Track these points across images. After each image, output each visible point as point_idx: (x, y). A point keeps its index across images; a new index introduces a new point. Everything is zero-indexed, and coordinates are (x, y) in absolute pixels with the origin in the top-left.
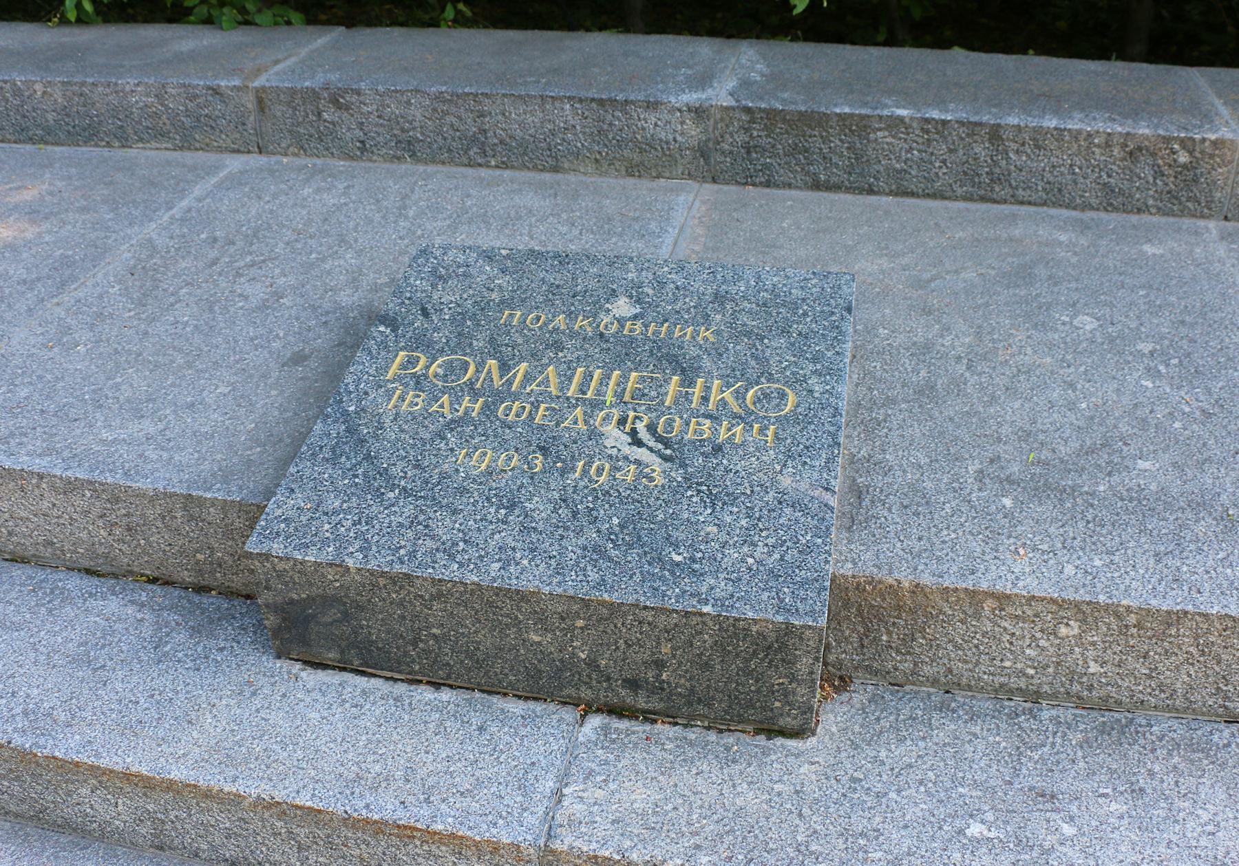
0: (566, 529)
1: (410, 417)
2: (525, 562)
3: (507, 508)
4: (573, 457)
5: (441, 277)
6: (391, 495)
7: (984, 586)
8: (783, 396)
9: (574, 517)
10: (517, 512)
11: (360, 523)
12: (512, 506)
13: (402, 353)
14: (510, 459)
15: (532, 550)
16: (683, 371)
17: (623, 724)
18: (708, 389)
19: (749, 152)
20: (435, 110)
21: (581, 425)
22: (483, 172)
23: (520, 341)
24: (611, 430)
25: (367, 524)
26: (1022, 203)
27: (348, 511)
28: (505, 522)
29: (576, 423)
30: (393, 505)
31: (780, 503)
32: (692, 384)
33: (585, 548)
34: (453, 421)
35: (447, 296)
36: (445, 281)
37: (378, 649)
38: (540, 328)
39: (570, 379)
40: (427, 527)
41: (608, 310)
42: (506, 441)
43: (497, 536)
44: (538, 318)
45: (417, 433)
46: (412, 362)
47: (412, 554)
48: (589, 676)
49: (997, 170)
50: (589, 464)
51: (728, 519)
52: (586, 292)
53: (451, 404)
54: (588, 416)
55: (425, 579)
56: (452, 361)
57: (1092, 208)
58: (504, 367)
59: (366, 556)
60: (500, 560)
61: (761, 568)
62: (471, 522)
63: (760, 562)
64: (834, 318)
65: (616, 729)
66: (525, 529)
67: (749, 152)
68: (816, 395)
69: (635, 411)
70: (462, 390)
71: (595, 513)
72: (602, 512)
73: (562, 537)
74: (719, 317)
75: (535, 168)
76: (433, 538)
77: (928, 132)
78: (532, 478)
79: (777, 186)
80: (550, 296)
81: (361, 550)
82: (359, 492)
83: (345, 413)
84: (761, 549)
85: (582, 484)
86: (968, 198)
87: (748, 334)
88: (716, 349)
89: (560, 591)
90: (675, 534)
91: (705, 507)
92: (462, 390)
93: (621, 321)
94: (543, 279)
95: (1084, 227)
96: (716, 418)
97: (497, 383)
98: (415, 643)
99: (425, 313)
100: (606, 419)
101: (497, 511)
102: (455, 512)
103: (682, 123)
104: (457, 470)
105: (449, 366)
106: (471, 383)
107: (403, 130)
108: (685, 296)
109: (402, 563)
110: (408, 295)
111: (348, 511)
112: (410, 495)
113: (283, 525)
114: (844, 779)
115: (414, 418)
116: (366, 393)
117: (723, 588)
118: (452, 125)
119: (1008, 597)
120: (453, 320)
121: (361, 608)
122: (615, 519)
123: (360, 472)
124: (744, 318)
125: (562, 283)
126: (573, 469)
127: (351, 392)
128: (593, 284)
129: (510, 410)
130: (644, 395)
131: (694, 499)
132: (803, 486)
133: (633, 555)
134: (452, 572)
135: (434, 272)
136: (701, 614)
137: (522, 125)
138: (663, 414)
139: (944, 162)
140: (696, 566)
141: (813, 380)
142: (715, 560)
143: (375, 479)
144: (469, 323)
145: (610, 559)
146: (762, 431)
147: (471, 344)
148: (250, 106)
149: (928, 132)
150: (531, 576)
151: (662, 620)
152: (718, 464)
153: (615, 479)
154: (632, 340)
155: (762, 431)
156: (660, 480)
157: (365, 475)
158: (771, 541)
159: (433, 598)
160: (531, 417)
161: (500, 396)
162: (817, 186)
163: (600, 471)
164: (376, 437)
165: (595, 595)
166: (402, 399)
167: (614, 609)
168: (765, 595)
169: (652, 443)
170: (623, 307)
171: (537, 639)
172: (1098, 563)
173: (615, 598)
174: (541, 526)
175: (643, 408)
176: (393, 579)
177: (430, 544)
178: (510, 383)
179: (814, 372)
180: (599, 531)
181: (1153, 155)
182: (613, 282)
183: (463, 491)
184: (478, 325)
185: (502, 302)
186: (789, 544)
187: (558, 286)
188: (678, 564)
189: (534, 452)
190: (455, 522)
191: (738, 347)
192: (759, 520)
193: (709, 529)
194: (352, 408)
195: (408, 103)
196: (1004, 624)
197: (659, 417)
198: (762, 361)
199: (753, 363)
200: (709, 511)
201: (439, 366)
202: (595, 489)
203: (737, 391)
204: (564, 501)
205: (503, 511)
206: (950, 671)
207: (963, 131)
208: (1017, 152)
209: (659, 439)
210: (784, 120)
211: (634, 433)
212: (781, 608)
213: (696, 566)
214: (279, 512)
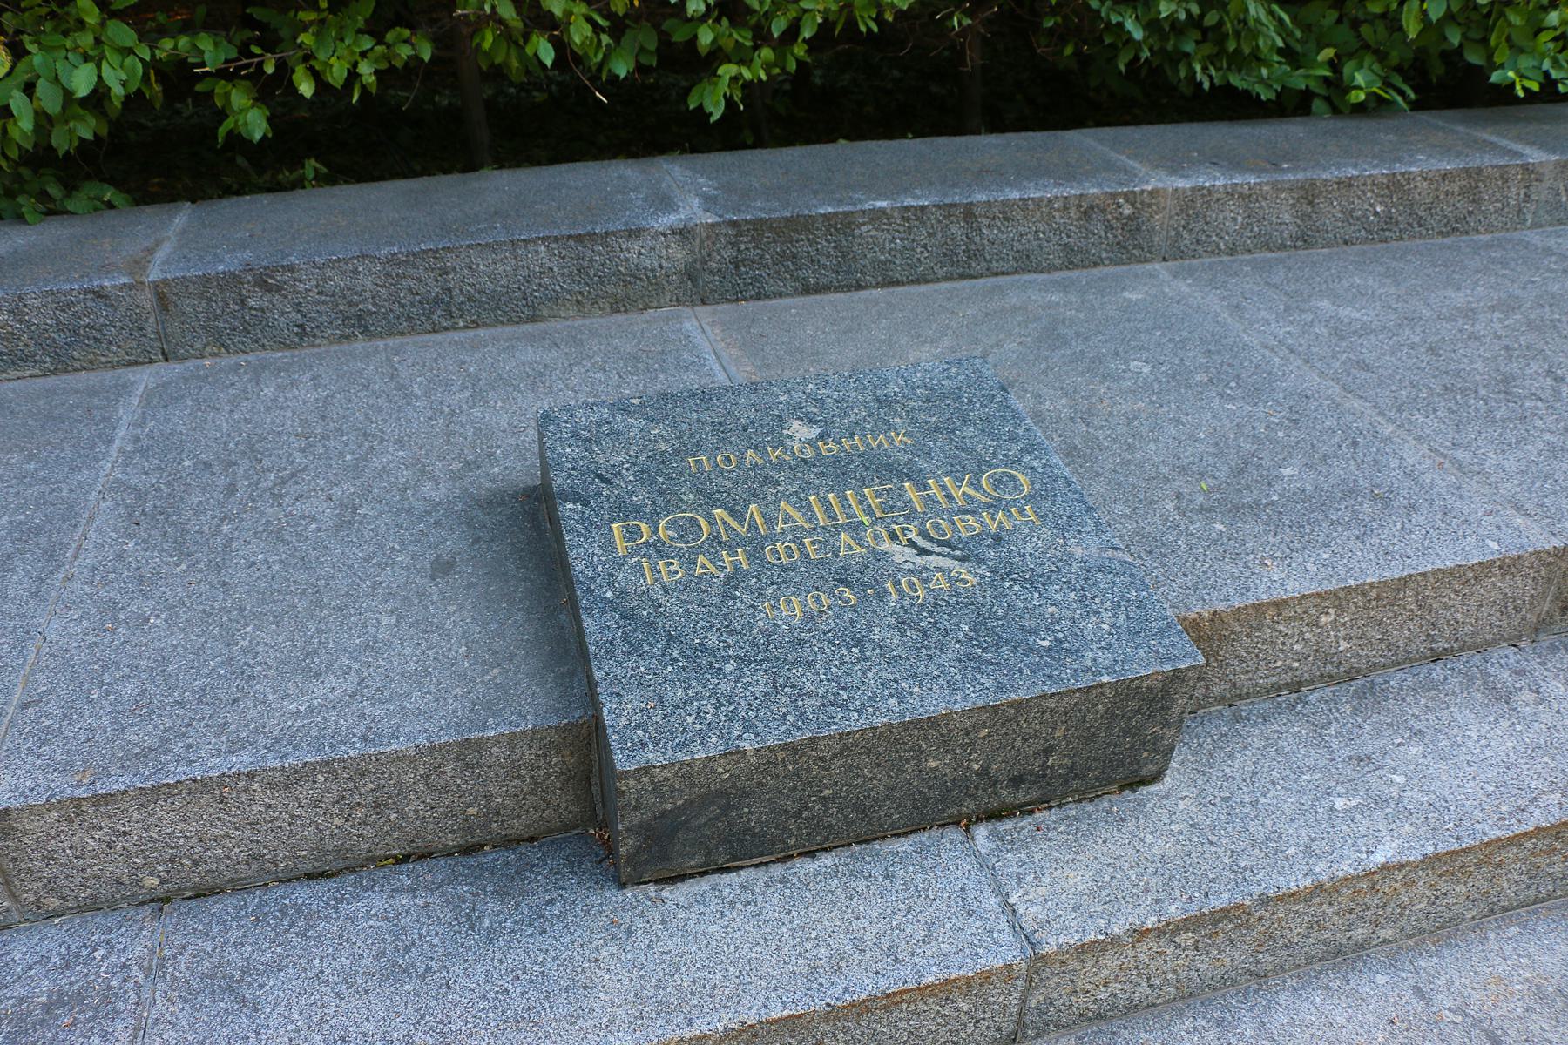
0: (928, 648)
2: (916, 689)
3: (856, 646)
5: (588, 440)
6: (728, 668)
7: (1265, 598)
8: (1013, 478)
13: (614, 526)
14: (818, 599)
15: (915, 677)
16: (910, 479)
17: (1007, 825)
18: (944, 487)
19: (737, 268)
20: (388, 275)
21: (858, 550)
22: (456, 336)
23: (729, 484)
24: (886, 546)
26: (996, 274)
28: (867, 660)
32: (926, 487)
35: (609, 456)
37: (754, 835)
39: (810, 508)
40: (793, 687)
43: (870, 675)
44: (728, 459)
47: (802, 716)
48: (977, 788)
49: (973, 247)
50: (896, 583)
51: (1058, 597)
55: (831, 737)
56: (675, 521)
57: (1057, 269)
58: (739, 516)
59: (757, 735)
60: (891, 696)
63: (1113, 626)
65: (1005, 831)
67: (737, 268)
73: (931, 657)
75: (510, 321)
76: (809, 695)
77: (908, 220)
79: (768, 297)
81: (746, 729)
83: (605, 600)
84: (1106, 616)
86: (948, 278)
87: (937, 430)
89: (969, 705)
90: (1026, 623)
94: (699, 420)
95: (1064, 287)
97: (743, 530)
98: (798, 815)
100: (876, 537)
103: (667, 248)
107: (351, 304)
109: (800, 729)
113: (640, 733)
114: (1217, 801)
117: (1104, 658)
118: (410, 290)
119: (1285, 602)
121: (746, 794)
123: (675, 654)
126: (886, 591)
132: (1095, 552)
133: (1006, 652)
134: (855, 722)
135: (575, 435)
136: (1102, 685)
137: (493, 277)
139: (925, 246)
141: (1026, 458)
146: (1021, 511)
148: (147, 305)
149: (908, 220)
150: (935, 702)
151: (1066, 703)
154: (838, 460)
155: (1021, 511)
156: (975, 581)
157: (683, 654)
158: (1107, 605)
159: (835, 755)
160: (805, 555)
161: (755, 545)
162: (807, 290)
163: (912, 586)
165: (1003, 698)
166: (655, 570)
167: (1020, 706)
168: (1141, 651)
169: (937, 549)
170: (800, 432)
171: (933, 764)
172: (1326, 556)
173: (1021, 695)
176: (794, 749)
177: (810, 701)
178: (753, 526)
179: (1021, 450)
181: (1103, 211)
183: (800, 643)
185: (676, 451)
188: (1050, 649)
193: (1050, 610)
195: (355, 271)
196: (1281, 628)
198: (970, 451)
206: (1234, 685)
207: (940, 214)
208: (989, 226)
209: (940, 544)
210: (771, 229)
211: (912, 544)
212: (1163, 660)
214: (623, 721)
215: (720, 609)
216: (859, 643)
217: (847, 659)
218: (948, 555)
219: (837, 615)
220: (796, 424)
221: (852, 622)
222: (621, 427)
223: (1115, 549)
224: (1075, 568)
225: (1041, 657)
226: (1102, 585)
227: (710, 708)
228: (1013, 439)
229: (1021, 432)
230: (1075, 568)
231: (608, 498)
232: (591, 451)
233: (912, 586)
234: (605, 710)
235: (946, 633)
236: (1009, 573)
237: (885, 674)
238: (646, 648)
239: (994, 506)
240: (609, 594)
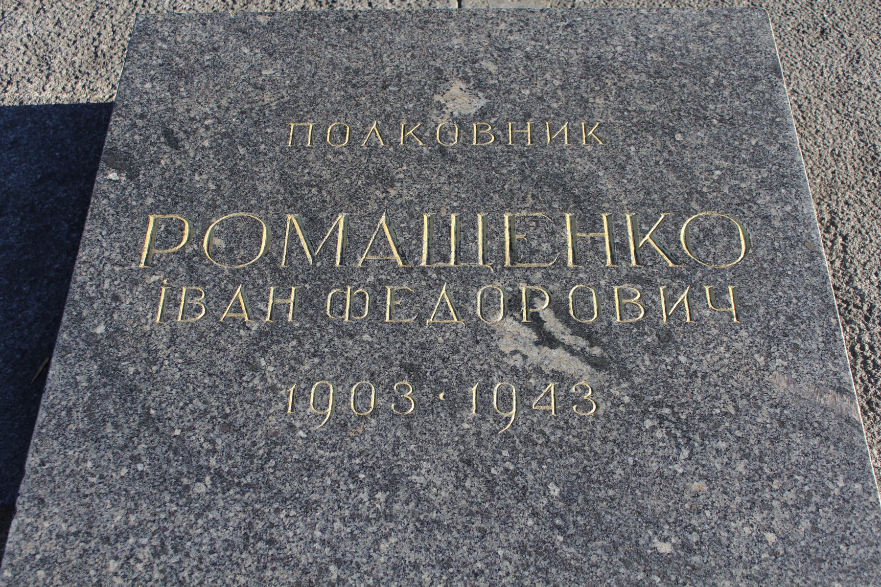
0: (485, 515)
1: (194, 336)
4: (459, 378)
5: (180, 73)
6: (200, 488)
8: (731, 231)
9: (491, 490)
10: (402, 494)
11: (164, 551)
12: (392, 485)
15: (445, 565)
23: (326, 175)
25: (176, 551)
27: (139, 529)
28: (390, 517)
29: (447, 314)
30: (208, 508)
31: (782, 424)
32: (596, 225)
33: (522, 550)
34: (262, 334)
35: (198, 105)
36: (189, 81)
38: (349, 146)
40: (271, 542)
41: (440, 107)
42: (351, 361)
43: (384, 546)
45: (212, 364)
46: (170, 233)
52: (399, 76)
53: (250, 302)
54: (462, 301)
56: (232, 223)
58: (315, 226)
61: (791, 550)
62: (338, 525)
64: (760, 87)
66: (425, 526)
68: (777, 223)
69: (529, 282)
70: (262, 275)
71: (519, 480)
72: (530, 476)
73: (483, 533)
74: (600, 101)
76: (286, 562)
78: (409, 426)
80: (350, 90)
82: (148, 490)
83: (91, 340)
84: (780, 515)
85: (485, 427)
87: (650, 126)
88: (614, 158)
90: (650, 502)
91: (678, 446)
92: (262, 275)
93: (462, 123)
96: (649, 282)
99: (173, 142)
100: (489, 302)
101: (372, 498)
102: (308, 508)
104: (291, 426)
105: (230, 231)
106: (271, 259)
108: (544, 71)
110: (139, 110)
111: (139, 529)
112: (230, 485)
113: (41, 573)
115: (201, 336)
116: (116, 298)
120: (217, 148)
122: (552, 486)
124: (638, 101)
125: (360, 65)
126: (466, 399)
127: (91, 299)
128: (406, 63)
129: (345, 301)
130: (533, 252)
131: (659, 434)
132: (806, 389)
135: (167, 64)
138: (570, 283)
140: (696, 559)
142: (719, 542)
143: (169, 461)
144: (242, 151)
145: (566, 565)
147: (254, 188)
152: (674, 365)
153: (533, 412)
156: (598, 408)
161: (320, 278)
163: (505, 398)
164: (149, 378)
166: (172, 300)
169: (568, 339)
170: (460, 100)
174: (446, 517)
175: (539, 275)
179: (762, 183)
180: (535, 514)
182: (434, 56)
183: (311, 466)
184: (256, 153)
185: (282, 107)
186: (816, 498)
187: (357, 72)
188: (668, 560)
189: (399, 377)
190: (313, 526)
191: (643, 151)
192: (761, 460)
194: (100, 329)
197: (565, 290)
199: (672, 177)
200: (685, 453)
201: (216, 234)
202: (507, 435)
203: (662, 229)
204: (468, 462)
205: (381, 496)
209: (579, 330)
211: (536, 322)
213: (696, 559)
214: (28, 549)
215: (228, 386)
216: (392, 485)
217: (363, 510)
218: (581, 354)
219: (382, 431)
220: (457, 87)
221: (397, 444)
222: (225, 57)
223: (841, 391)
224: (764, 415)
225: (648, 572)
226: (794, 457)
227: (145, 554)
228: (757, 162)
229: (773, 149)
230: (764, 415)
231: (164, 170)
232: (173, 90)
233: (505, 398)
234: (15, 523)
235: (523, 494)
236: (657, 404)
237: (405, 550)
238: (109, 429)
239: (683, 274)
240: (100, 329)
